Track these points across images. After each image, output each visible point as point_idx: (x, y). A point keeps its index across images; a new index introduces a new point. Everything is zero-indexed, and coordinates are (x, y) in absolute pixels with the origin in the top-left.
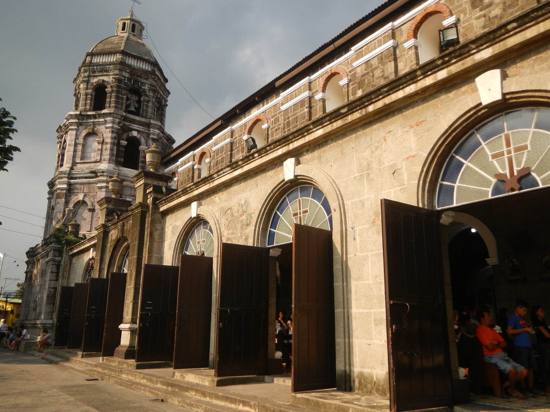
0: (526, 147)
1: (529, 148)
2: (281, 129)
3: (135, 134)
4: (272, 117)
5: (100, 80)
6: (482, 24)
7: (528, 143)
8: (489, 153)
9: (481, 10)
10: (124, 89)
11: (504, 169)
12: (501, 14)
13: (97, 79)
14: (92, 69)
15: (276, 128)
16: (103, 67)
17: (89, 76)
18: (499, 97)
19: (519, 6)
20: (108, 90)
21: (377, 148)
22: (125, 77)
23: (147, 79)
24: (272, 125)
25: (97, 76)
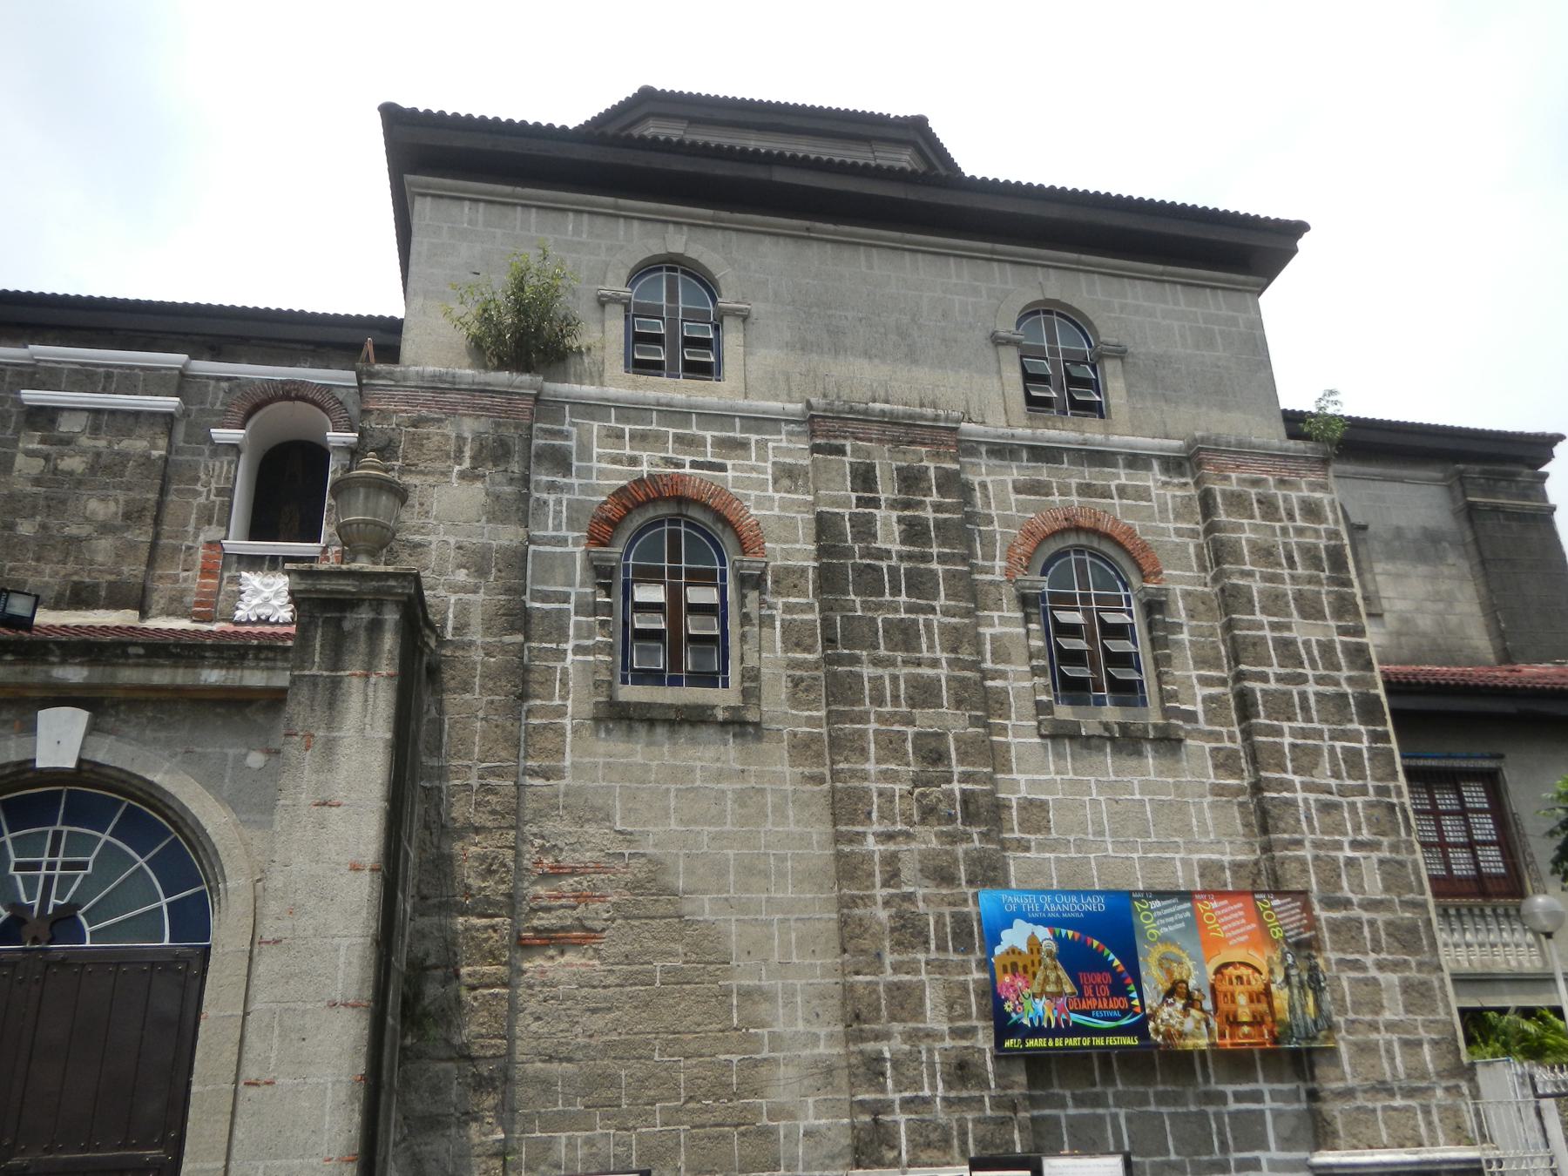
0: (84, 866)
1: (89, 870)
6: (35, 472)
7: (91, 859)
8: (14, 859)
9: (43, 441)
11: (31, 896)
12: (83, 474)
18: (71, 764)
19: (124, 479)
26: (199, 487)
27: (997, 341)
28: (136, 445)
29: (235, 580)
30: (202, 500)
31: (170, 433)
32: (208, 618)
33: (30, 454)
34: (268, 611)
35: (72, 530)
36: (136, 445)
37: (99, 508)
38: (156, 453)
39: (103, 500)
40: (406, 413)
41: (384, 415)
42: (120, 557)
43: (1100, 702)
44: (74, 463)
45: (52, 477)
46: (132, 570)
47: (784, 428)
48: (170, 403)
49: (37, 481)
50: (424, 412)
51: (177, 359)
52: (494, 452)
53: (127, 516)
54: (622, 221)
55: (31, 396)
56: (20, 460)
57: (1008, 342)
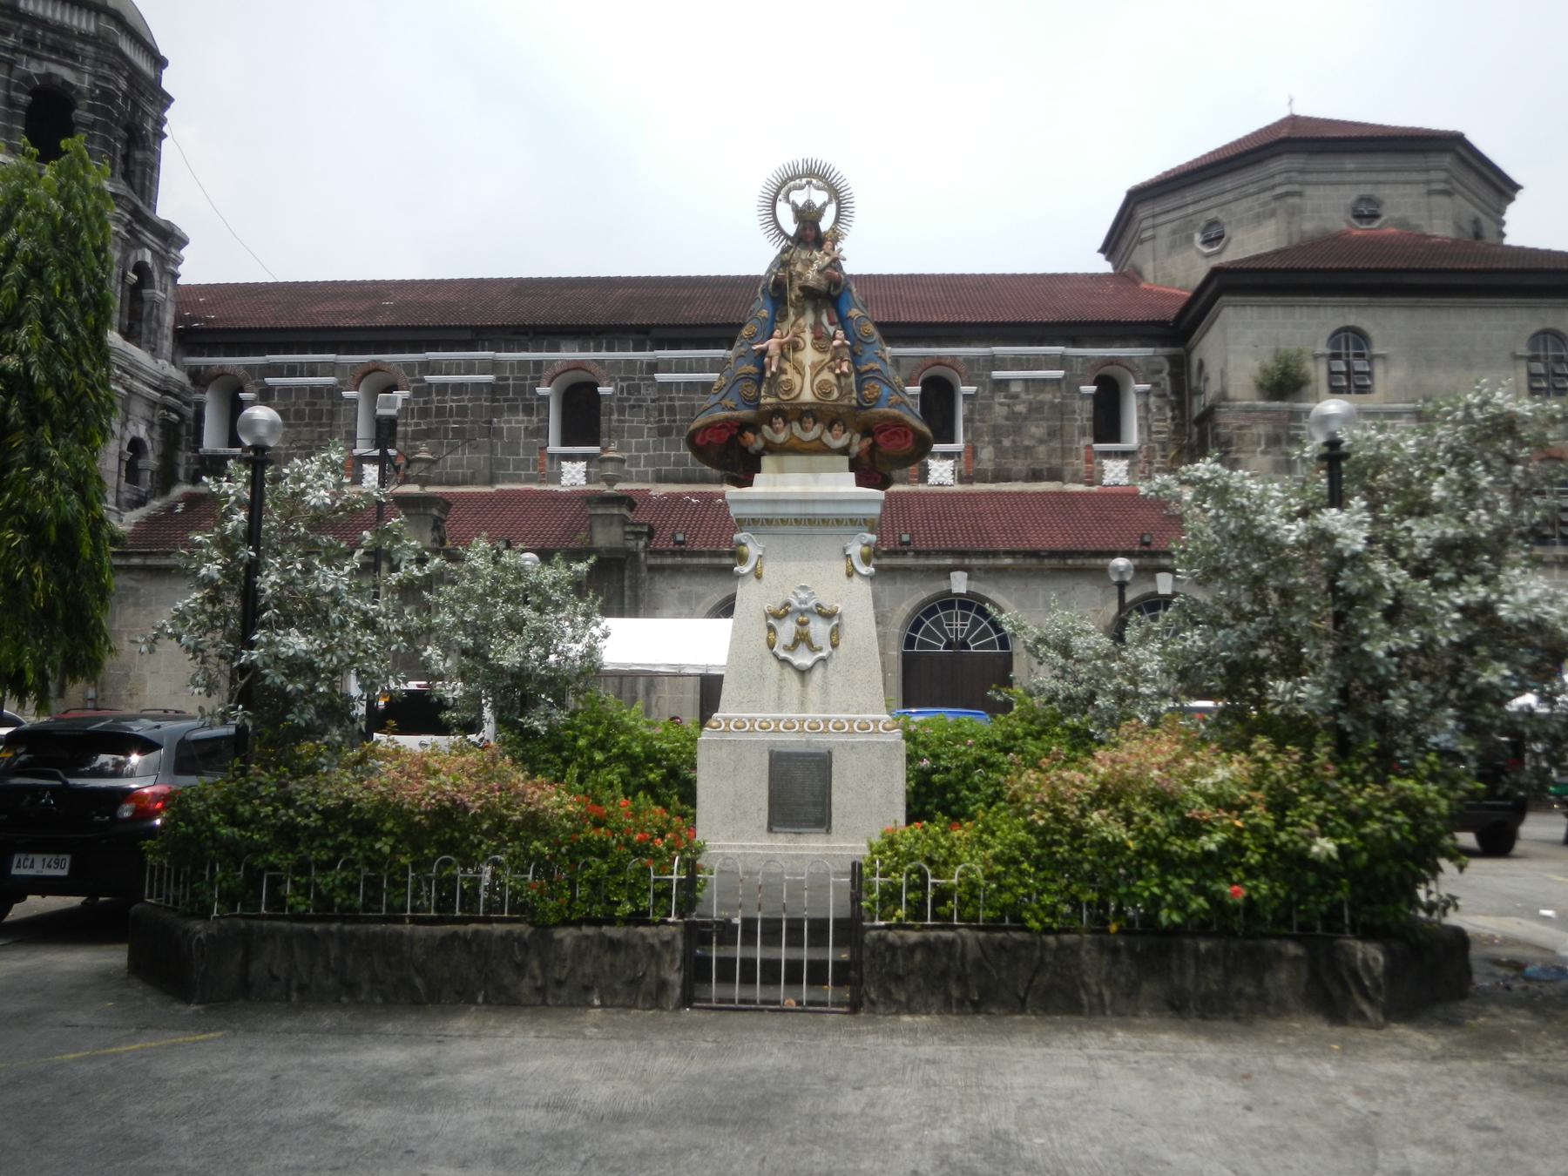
2: (648, 410)
3: (148, 257)
4: (623, 379)
5: (57, 76)
10: (117, 122)
13: (41, 65)
14: (25, 32)
15: (632, 403)
16: (64, 40)
17: (14, 50)
20: (82, 114)
21: (1065, 593)
22: (119, 89)
23: (152, 103)
24: (622, 392)
25: (40, 59)
26: (1077, 416)
27: (1516, 357)
28: (1046, 396)
29: (1100, 464)
30: (1079, 423)
31: (1060, 389)
32: (1090, 484)
33: (1001, 404)
34: (1116, 480)
35: (1026, 443)
36: (1046, 396)
37: (1037, 430)
38: (1057, 401)
39: (1037, 426)
40: (1235, 423)
41: (1226, 426)
42: (1050, 456)
43: (1554, 544)
44: (1021, 408)
45: (1012, 416)
46: (1055, 462)
47: (1406, 416)
48: (1059, 374)
49: (1007, 419)
50: (1242, 423)
51: (1058, 350)
52: (1274, 441)
53: (1049, 434)
54: (1322, 309)
55: (997, 374)
56: (997, 408)
57: (1522, 357)
